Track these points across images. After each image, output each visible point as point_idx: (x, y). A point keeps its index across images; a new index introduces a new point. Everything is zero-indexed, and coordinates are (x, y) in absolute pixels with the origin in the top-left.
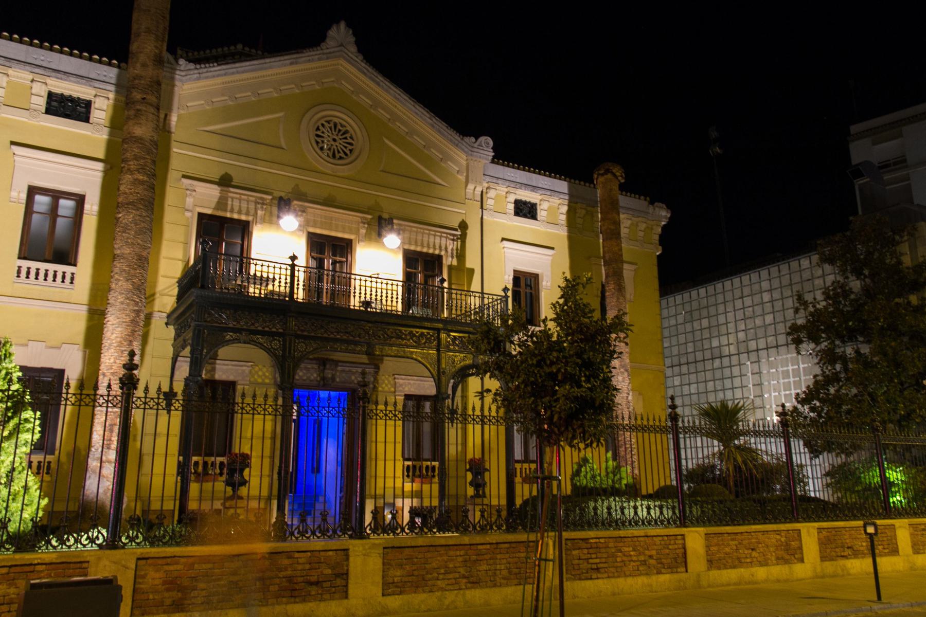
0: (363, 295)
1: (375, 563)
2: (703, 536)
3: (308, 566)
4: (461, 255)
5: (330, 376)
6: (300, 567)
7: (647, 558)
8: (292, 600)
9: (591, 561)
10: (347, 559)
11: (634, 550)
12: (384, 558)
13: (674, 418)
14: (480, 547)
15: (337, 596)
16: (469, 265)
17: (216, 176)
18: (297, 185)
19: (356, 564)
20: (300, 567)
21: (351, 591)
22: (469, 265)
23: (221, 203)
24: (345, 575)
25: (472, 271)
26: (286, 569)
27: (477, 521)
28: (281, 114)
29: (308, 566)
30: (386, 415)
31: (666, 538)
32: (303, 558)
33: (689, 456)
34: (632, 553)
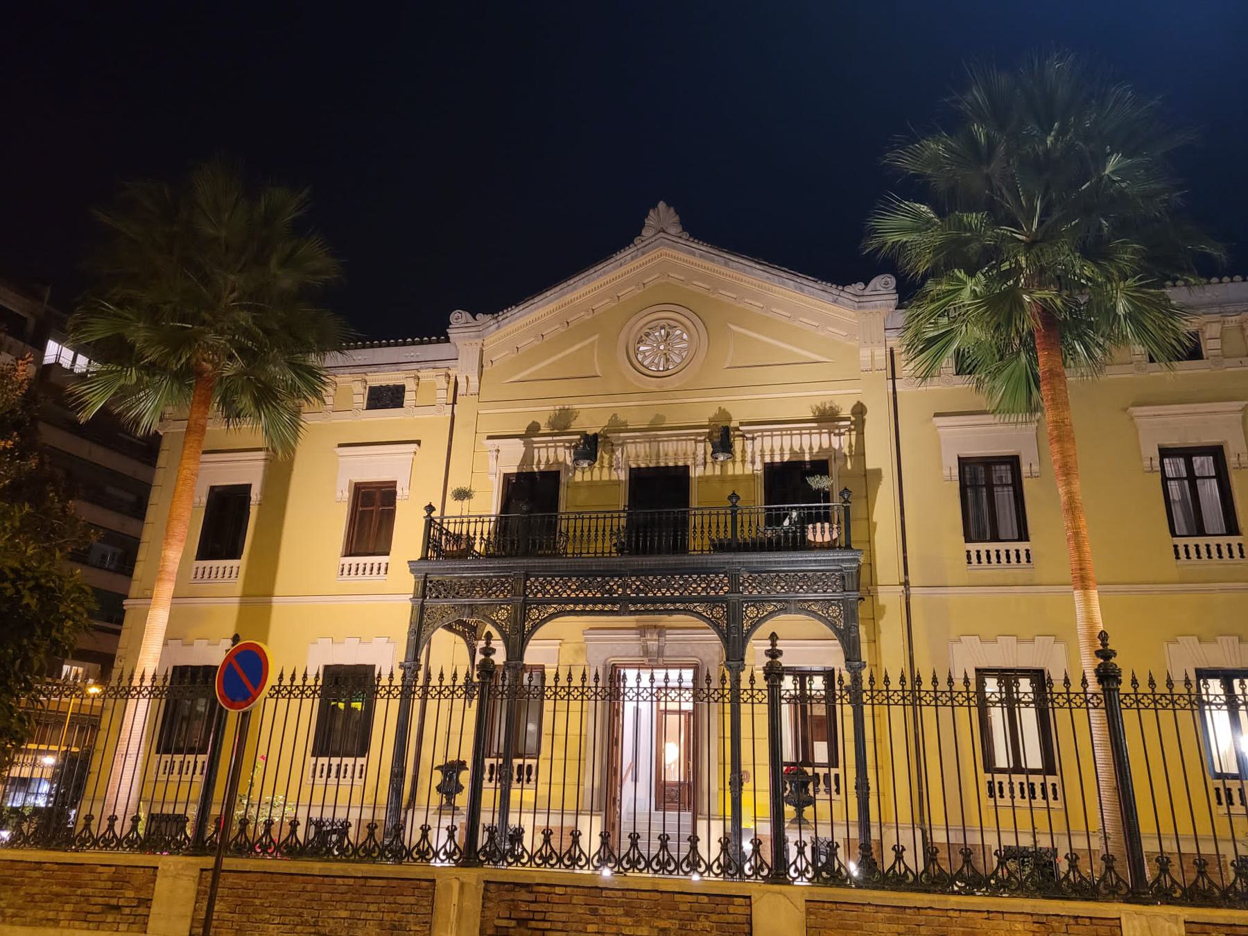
2: (802, 905)
3: (109, 884)
4: (859, 452)
5: (655, 648)
6: (101, 885)
8: (85, 925)
9: (533, 924)
11: (627, 914)
12: (199, 884)
13: (1108, 675)
14: (339, 881)
15: (135, 927)
16: (870, 465)
17: (522, 430)
18: (615, 415)
19: (162, 886)
20: (101, 885)
21: (150, 924)
22: (870, 465)
23: (527, 458)
24: (146, 902)
25: (878, 473)
26: (86, 886)
27: (441, 845)
28: (596, 337)
29: (109, 884)
30: (1155, 702)
31: (706, 899)
34: (623, 920)
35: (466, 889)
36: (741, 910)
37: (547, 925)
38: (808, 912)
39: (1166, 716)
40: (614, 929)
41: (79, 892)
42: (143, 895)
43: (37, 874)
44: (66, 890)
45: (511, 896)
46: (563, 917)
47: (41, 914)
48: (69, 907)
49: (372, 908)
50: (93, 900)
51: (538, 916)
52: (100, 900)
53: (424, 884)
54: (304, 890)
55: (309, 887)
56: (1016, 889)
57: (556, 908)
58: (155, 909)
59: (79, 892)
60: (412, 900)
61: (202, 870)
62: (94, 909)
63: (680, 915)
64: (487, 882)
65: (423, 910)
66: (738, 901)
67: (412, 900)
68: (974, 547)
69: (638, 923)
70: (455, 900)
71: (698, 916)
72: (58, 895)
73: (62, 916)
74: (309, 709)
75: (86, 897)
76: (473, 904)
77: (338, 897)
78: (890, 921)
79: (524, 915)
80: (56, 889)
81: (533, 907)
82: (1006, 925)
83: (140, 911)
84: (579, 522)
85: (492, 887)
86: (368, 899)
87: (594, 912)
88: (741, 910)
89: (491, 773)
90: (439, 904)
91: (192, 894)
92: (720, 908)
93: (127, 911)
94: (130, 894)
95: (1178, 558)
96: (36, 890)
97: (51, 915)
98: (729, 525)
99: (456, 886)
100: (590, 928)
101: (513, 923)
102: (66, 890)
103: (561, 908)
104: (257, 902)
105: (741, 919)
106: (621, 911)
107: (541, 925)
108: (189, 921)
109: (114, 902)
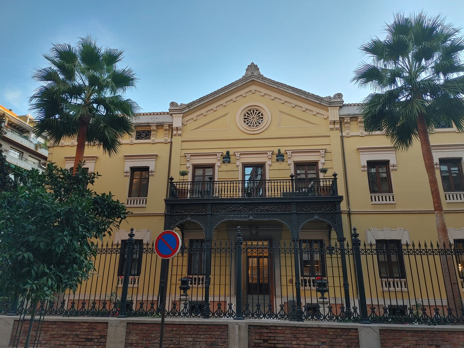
0: (282, 190)
1: (122, 330)
3: (87, 330)
6: (83, 330)
7: (320, 343)
10: (107, 328)
19: (111, 330)
20: (83, 330)
24: (105, 337)
29: (87, 330)
32: (85, 325)
33: (180, 268)
34: (307, 339)
35: (241, 328)
36: (354, 334)
37: (276, 342)
38: (380, 334)
39: (431, 257)
40: (304, 343)
41: (74, 333)
42: (102, 334)
43: (54, 326)
44: (68, 333)
45: (260, 331)
46: (283, 339)
47: (58, 343)
48: (70, 340)
49: (202, 337)
50: (81, 337)
51: (271, 338)
52: (83, 337)
53: (223, 327)
54: (172, 330)
55: (175, 329)
56: (456, 323)
57: (279, 335)
58: (108, 339)
59: (74, 333)
60: (219, 333)
61: (127, 323)
62: (81, 340)
63: (330, 337)
64: (249, 325)
65: (224, 337)
66: (352, 331)
67: (219, 333)
68: (373, 195)
69: (313, 340)
70: (237, 333)
71: (337, 337)
72: (64, 335)
73: (67, 343)
74: (115, 258)
75: (77, 335)
76: (245, 334)
77: (187, 333)
78: (412, 336)
79: (266, 338)
80: (63, 332)
81: (269, 335)
82: (456, 336)
83: (102, 340)
84: (232, 185)
85: (252, 328)
86: (200, 333)
87: (295, 337)
88: (354, 334)
89: (314, 283)
90: (231, 335)
91: (124, 333)
92: (345, 334)
93: (96, 340)
94: (97, 334)
95: (446, 199)
96: (55, 333)
97: (62, 343)
98: (291, 186)
99: (237, 327)
100: (294, 343)
101: (262, 341)
102: (68, 333)
103: (281, 335)
104: (153, 335)
105: (354, 337)
106: (306, 336)
107: (273, 342)
108: (124, 343)
109: (90, 337)
